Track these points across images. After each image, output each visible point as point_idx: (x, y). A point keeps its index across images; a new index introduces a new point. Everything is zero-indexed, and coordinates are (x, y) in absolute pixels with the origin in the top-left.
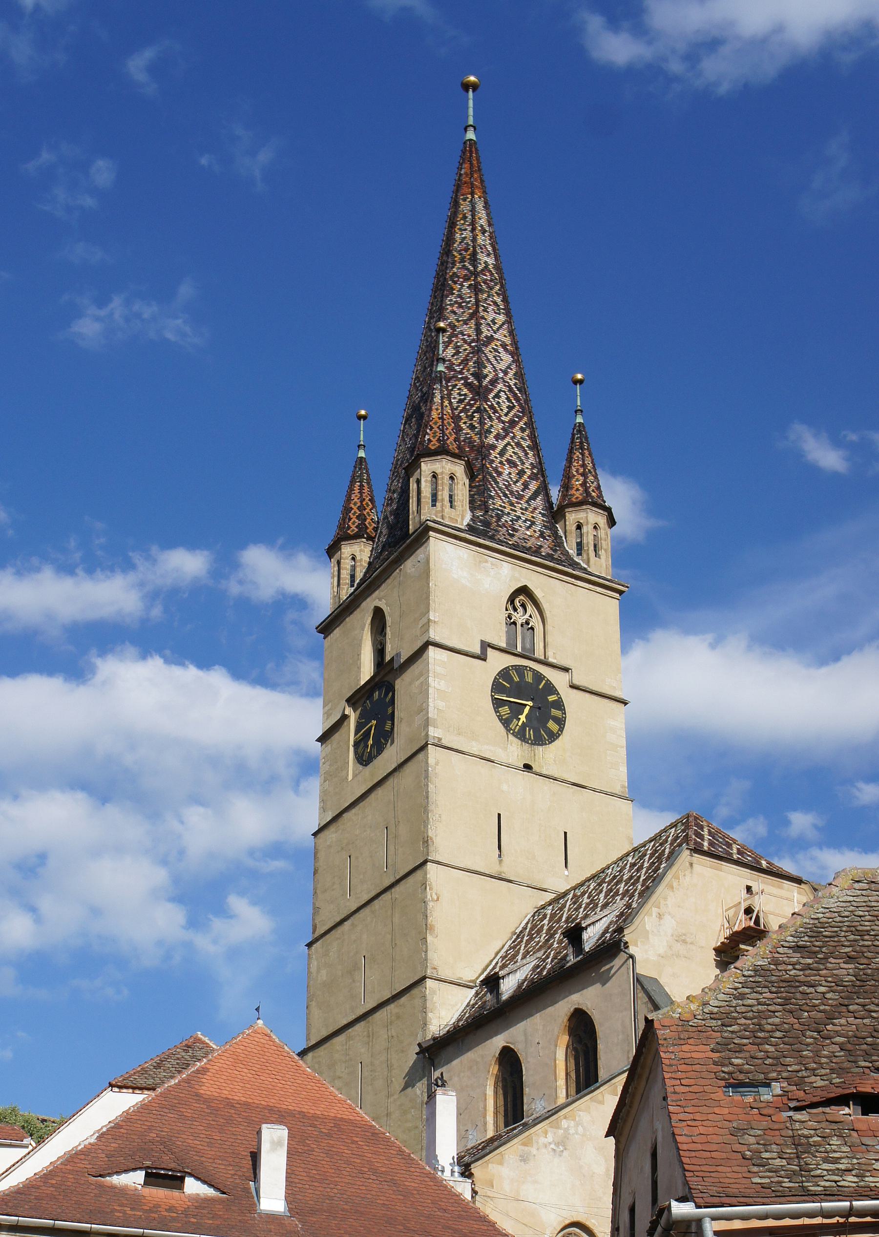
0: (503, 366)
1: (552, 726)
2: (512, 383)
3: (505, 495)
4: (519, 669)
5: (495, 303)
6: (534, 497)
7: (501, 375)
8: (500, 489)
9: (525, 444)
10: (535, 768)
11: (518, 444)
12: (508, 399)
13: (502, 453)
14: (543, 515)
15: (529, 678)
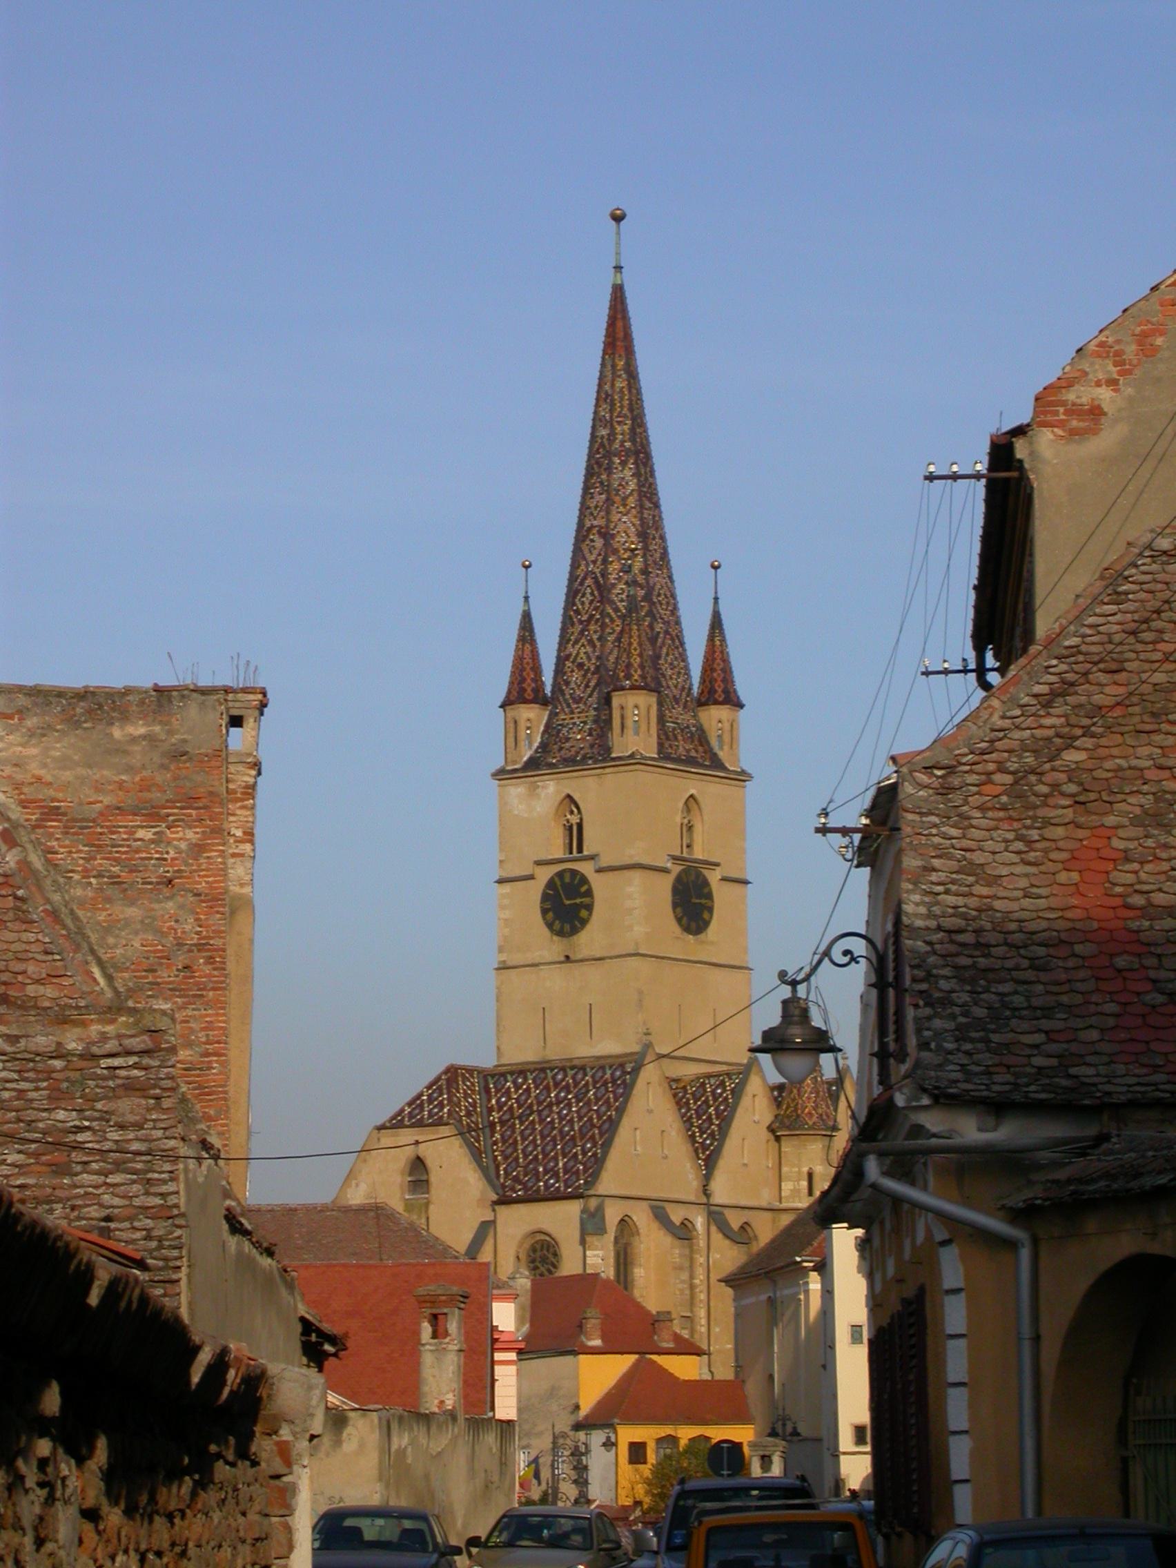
0: (593, 558)
1: (584, 913)
2: (597, 571)
3: (569, 706)
4: (560, 875)
5: (601, 483)
6: (590, 696)
7: (591, 567)
8: (566, 700)
9: (595, 637)
10: (572, 957)
11: (591, 642)
12: (592, 594)
13: (573, 662)
14: (595, 709)
15: (567, 880)
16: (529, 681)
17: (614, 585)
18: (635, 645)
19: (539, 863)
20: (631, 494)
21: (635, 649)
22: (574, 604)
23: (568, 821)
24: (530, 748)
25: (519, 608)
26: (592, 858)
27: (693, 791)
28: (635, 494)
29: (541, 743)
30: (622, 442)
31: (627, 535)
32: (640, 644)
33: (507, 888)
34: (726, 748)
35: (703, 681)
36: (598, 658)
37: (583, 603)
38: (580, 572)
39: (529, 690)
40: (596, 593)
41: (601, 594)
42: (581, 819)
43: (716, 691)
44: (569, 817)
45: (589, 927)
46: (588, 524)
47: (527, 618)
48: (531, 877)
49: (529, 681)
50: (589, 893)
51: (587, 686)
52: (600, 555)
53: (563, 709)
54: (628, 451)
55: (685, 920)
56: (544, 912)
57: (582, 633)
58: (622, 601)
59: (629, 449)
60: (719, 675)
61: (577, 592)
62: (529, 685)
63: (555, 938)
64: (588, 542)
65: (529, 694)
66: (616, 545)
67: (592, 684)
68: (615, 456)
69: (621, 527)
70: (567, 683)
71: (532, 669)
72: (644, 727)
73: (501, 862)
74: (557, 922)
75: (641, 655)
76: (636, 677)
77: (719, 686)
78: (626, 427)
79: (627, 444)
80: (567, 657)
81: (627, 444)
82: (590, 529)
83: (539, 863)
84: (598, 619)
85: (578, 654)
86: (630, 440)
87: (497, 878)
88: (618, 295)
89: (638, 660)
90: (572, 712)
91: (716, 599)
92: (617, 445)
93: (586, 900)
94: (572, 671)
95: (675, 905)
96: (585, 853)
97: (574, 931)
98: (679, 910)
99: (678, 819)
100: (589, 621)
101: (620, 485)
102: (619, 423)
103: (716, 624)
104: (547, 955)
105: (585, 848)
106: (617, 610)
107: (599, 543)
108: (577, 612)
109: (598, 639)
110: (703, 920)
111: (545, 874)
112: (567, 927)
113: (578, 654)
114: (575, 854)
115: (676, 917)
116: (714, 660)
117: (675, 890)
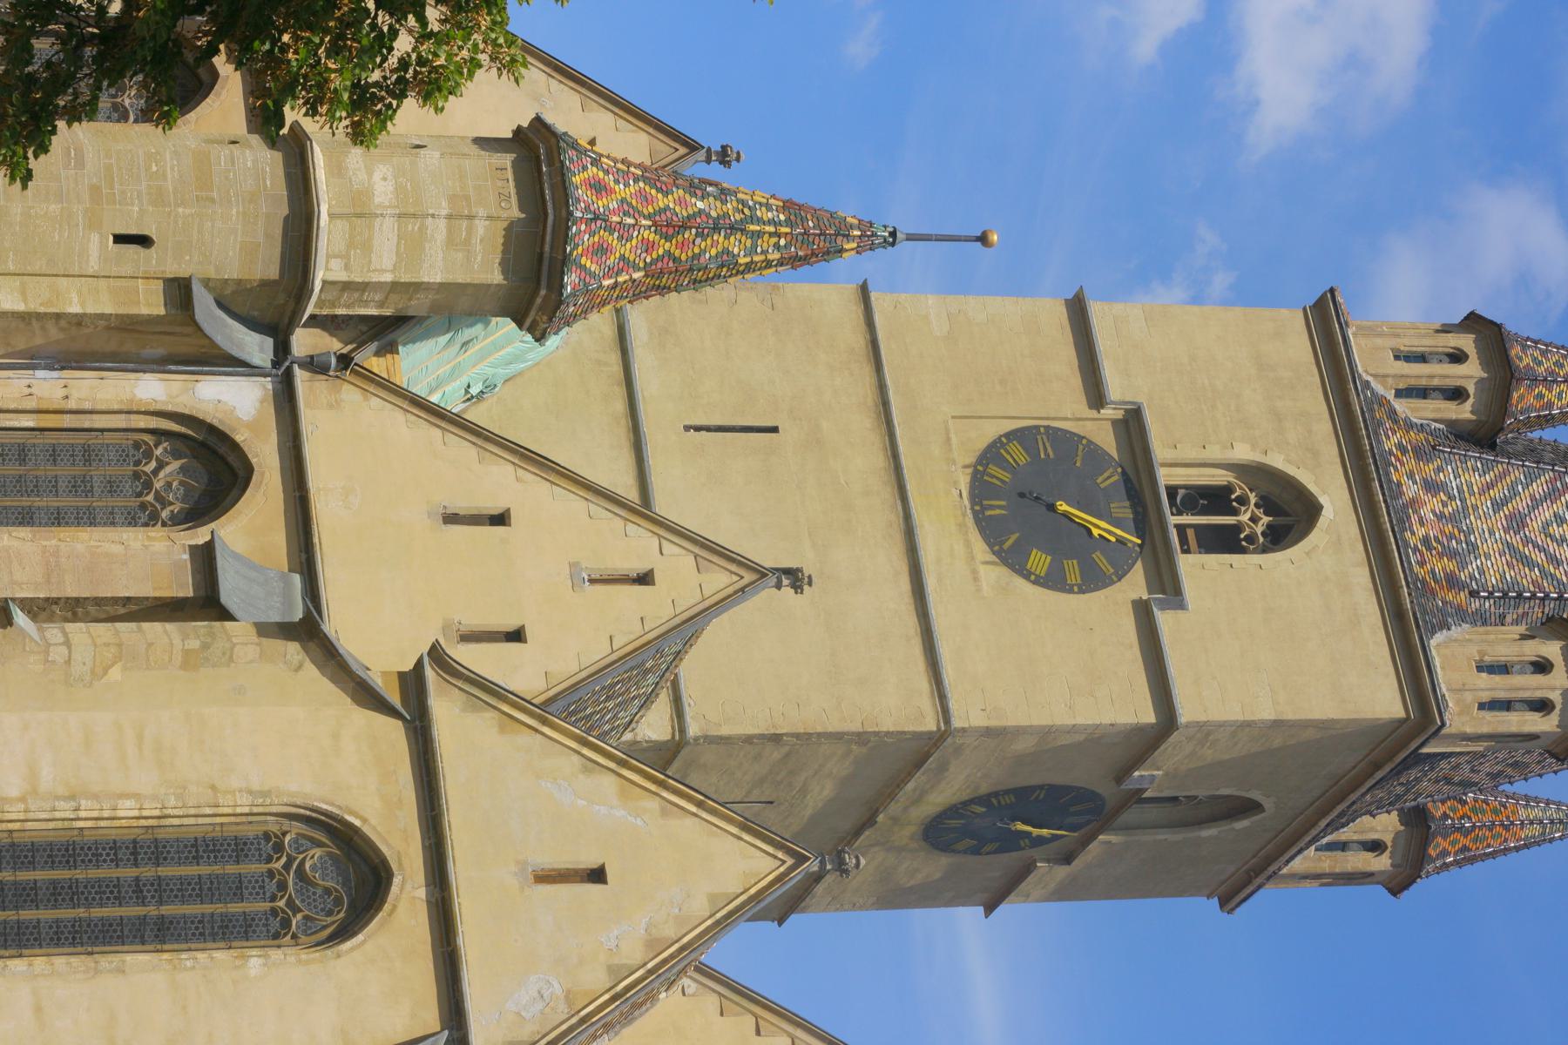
1: (1039, 561)
24: (1399, 394)
50: (1093, 581)
56: (1023, 436)
74: (1006, 476)
93: (1072, 570)
97: (990, 530)
98: (1011, 799)
115: (996, 794)
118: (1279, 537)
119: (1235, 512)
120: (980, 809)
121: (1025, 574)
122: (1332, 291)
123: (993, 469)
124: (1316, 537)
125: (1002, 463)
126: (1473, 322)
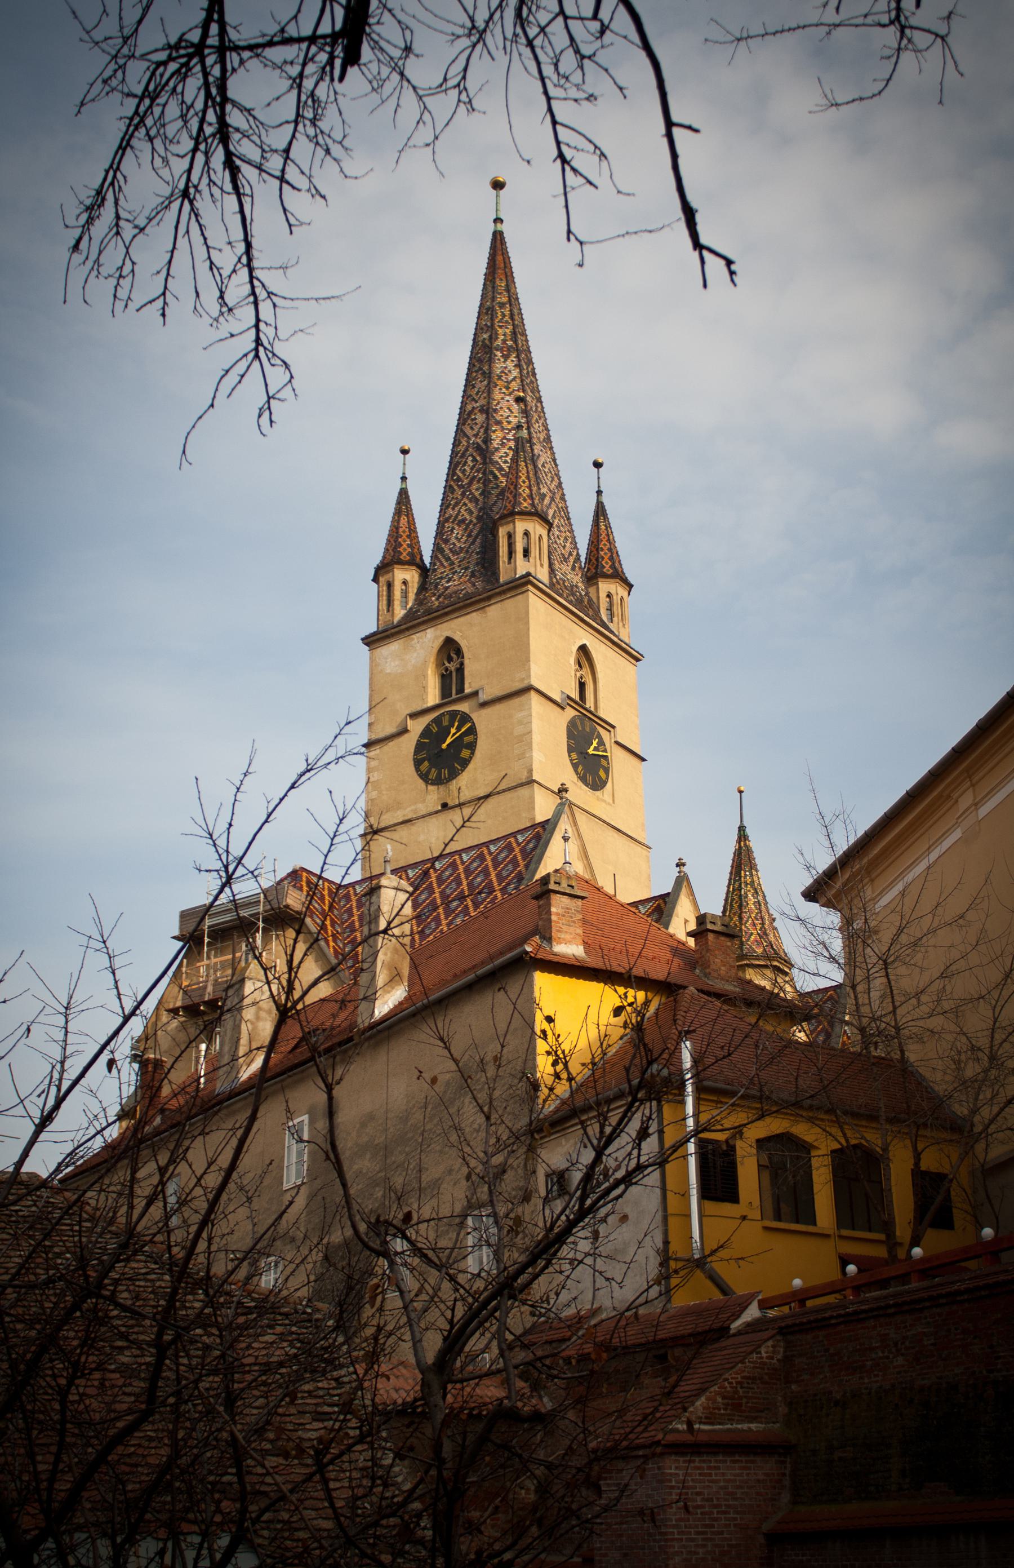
1: (465, 753)
2: (479, 441)
3: (448, 559)
4: (437, 721)
5: (484, 373)
6: (473, 543)
9: (477, 494)
10: (451, 804)
12: (474, 460)
14: (477, 553)
16: (405, 546)
17: (497, 449)
18: (523, 478)
19: (413, 716)
20: (514, 379)
21: (524, 482)
22: (454, 474)
23: (447, 669)
25: (398, 485)
26: (475, 694)
27: (584, 642)
28: (518, 381)
29: (416, 600)
30: (504, 341)
31: (510, 411)
32: (528, 477)
33: (375, 752)
34: (615, 619)
35: (589, 552)
36: (481, 509)
37: (464, 472)
38: (461, 448)
39: (405, 554)
40: (478, 458)
41: (484, 458)
42: (462, 664)
43: (604, 567)
44: (447, 665)
45: (471, 766)
46: (469, 407)
47: (403, 498)
48: (404, 731)
49: (405, 546)
50: (472, 731)
51: (469, 536)
52: (482, 427)
53: (442, 565)
54: (509, 348)
55: (580, 768)
56: (418, 763)
57: (463, 494)
58: (506, 462)
59: (511, 346)
60: (605, 554)
61: (458, 463)
62: (405, 549)
63: (430, 787)
64: (469, 422)
65: (404, 556)
66: (499, 418)
67: (475, 532)
68: (497, 350)
69: (504, 404)
70: (446, 541)
71: (409, 536)
72: (534, 552)
73: (370, 725)
74: (433, 770)
75: (530, 487)
76: (525, 504)
77: (607, 563)
78: (508, 331)
79: (510, 343)
80: (447, 520)
81: (510, 343)
82: (471, 413)
83: (413, 716)
84: (480, 479)
85: (459, 511)
86: (511, 340)
87: (366, 741)
88: (498, 241)
89: (527, 491)
90: (453, 563)
91: (599, 493)
92: (499, 342)
94: (453, 528)
95: (570, 750)
96: (468, 690)
97: (454, 775)
98: (574, 756)
99: (573, 673)
100: (470, 483)
101: (502, 372)
102: (501, 327)
103: (600, 512)
104: (422, 809)
105: (466, 686)
106: (501, 469)
107: (480, 418)
108: (459, 479)
109: (480, 494)
110: (600, 777)
111: (416, 727)
112: (445, 772)
113: (459, 511)
114: (454, 696)
115: (571, 760)
116: (598, 541)
117: (570, 735)
118: (459, 652)
119: (451, 672)
120: (580, 768)
121: (471, 758)
122: (363, 639)
123: (430, 777)
124: (456, 638)
125: (428, 772)
126: (375, 579)
